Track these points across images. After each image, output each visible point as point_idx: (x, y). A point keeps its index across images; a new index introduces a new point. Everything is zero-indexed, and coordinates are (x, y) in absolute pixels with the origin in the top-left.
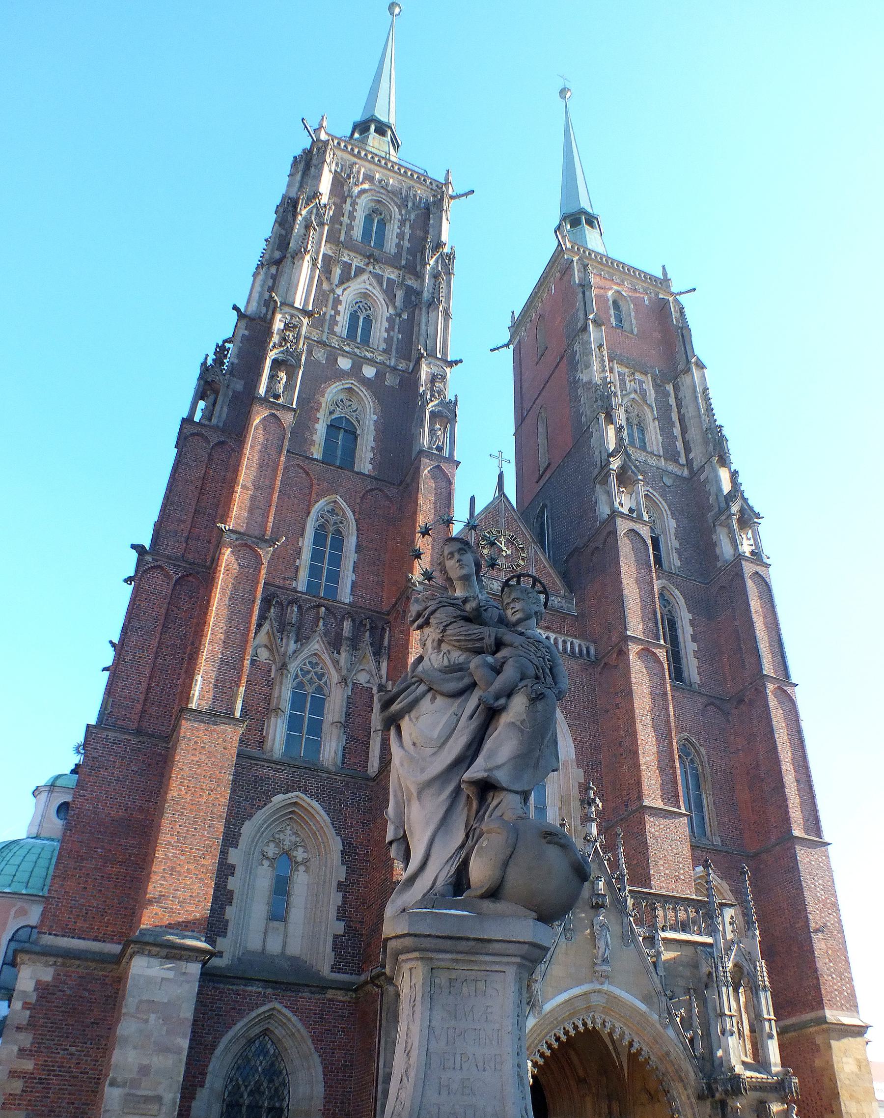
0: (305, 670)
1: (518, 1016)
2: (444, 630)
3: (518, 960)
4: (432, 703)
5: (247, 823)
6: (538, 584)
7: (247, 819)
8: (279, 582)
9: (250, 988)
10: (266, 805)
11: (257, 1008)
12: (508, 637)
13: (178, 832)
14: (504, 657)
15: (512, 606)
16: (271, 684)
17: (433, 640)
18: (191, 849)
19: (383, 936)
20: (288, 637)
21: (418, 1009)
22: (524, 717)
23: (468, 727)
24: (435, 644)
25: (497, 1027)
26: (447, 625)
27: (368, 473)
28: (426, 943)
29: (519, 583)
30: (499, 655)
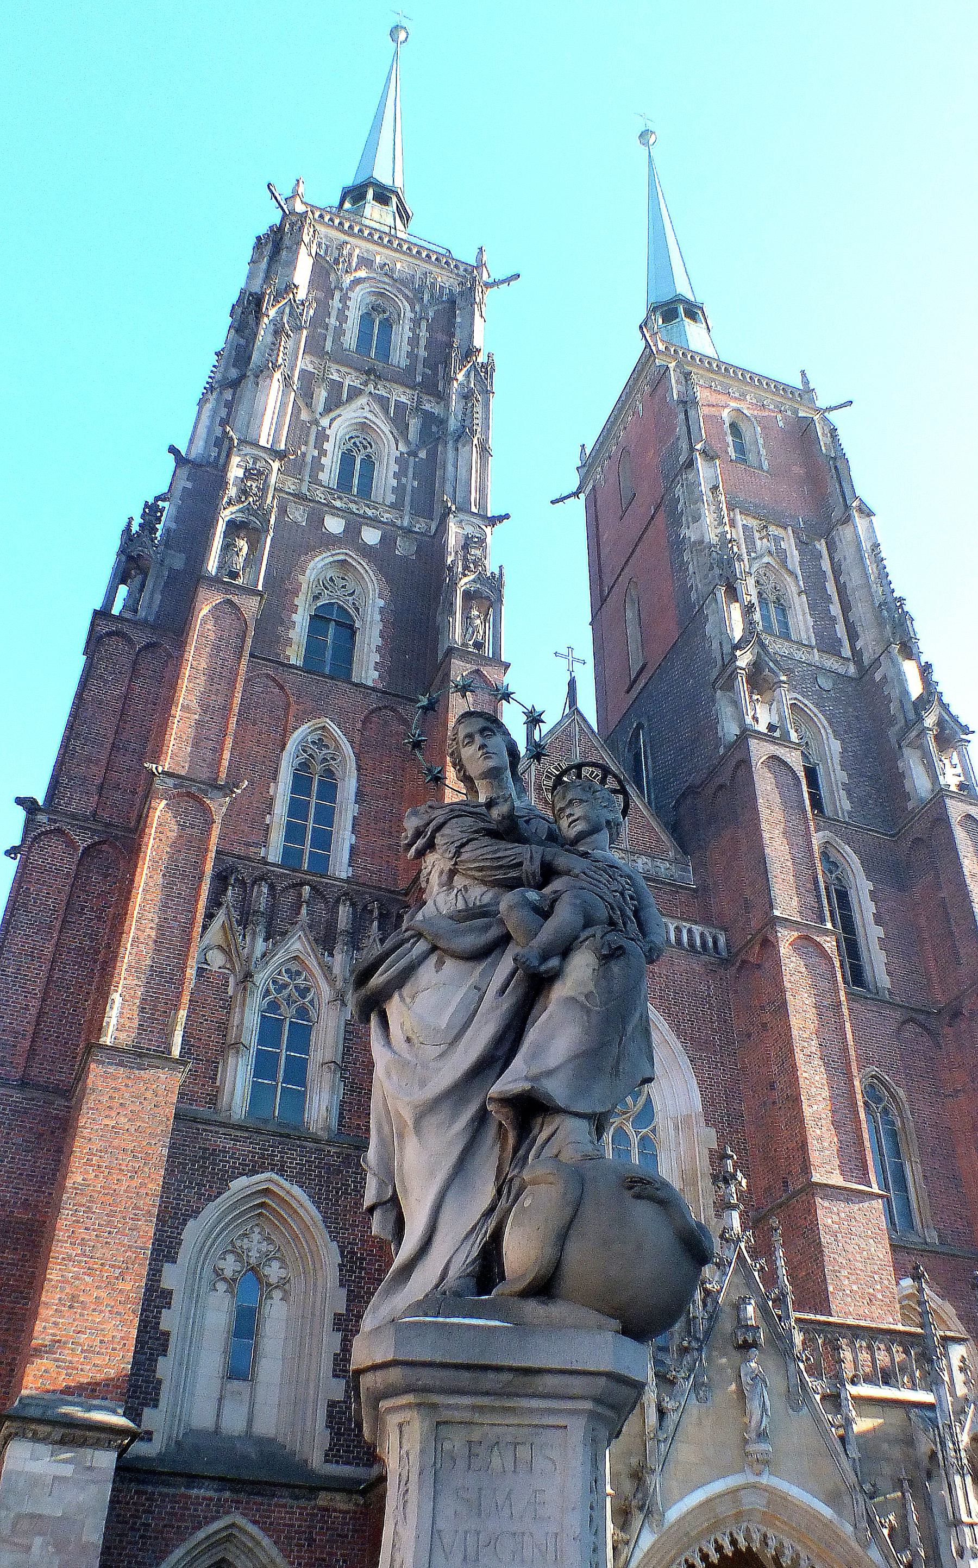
0: (281, 982)
1: (592, 1508)
2: (458, 853)
3: (588, 1405)
4: (437, 972)
5: (191, 1223)
6: (610, 779)
7: (191, 1216)
8: (239, 850)
9: (195, 1492)
10: (220, 1194)
11: (207, 1523)
12: (563, 860)
13: (83, 1239)
14: (556, 892)
15: (568, 812)
16: (228, 1006)
17: (441, 873)
18: (102, 1264)
19: (352, 1367)
20: (254, 933)
21: (413, 1496)
22: (591, 987)
23: (497, 1007)
24: (444, 877)
25: (553, 1529)
26: (463, 845)
27: (372, 685)
28: (426, 1377)
29: (579, 776)
30: (547, 890)
